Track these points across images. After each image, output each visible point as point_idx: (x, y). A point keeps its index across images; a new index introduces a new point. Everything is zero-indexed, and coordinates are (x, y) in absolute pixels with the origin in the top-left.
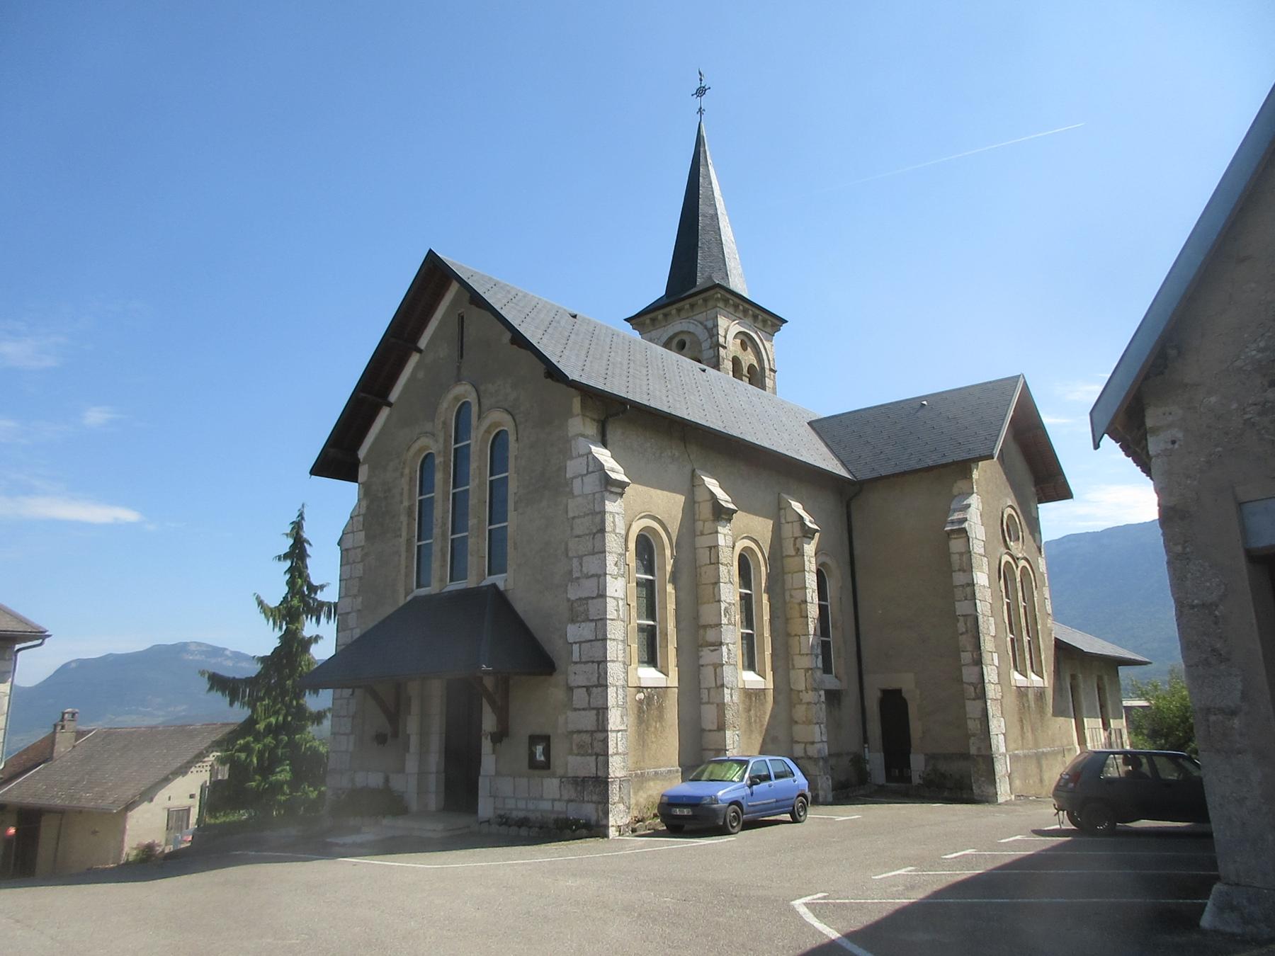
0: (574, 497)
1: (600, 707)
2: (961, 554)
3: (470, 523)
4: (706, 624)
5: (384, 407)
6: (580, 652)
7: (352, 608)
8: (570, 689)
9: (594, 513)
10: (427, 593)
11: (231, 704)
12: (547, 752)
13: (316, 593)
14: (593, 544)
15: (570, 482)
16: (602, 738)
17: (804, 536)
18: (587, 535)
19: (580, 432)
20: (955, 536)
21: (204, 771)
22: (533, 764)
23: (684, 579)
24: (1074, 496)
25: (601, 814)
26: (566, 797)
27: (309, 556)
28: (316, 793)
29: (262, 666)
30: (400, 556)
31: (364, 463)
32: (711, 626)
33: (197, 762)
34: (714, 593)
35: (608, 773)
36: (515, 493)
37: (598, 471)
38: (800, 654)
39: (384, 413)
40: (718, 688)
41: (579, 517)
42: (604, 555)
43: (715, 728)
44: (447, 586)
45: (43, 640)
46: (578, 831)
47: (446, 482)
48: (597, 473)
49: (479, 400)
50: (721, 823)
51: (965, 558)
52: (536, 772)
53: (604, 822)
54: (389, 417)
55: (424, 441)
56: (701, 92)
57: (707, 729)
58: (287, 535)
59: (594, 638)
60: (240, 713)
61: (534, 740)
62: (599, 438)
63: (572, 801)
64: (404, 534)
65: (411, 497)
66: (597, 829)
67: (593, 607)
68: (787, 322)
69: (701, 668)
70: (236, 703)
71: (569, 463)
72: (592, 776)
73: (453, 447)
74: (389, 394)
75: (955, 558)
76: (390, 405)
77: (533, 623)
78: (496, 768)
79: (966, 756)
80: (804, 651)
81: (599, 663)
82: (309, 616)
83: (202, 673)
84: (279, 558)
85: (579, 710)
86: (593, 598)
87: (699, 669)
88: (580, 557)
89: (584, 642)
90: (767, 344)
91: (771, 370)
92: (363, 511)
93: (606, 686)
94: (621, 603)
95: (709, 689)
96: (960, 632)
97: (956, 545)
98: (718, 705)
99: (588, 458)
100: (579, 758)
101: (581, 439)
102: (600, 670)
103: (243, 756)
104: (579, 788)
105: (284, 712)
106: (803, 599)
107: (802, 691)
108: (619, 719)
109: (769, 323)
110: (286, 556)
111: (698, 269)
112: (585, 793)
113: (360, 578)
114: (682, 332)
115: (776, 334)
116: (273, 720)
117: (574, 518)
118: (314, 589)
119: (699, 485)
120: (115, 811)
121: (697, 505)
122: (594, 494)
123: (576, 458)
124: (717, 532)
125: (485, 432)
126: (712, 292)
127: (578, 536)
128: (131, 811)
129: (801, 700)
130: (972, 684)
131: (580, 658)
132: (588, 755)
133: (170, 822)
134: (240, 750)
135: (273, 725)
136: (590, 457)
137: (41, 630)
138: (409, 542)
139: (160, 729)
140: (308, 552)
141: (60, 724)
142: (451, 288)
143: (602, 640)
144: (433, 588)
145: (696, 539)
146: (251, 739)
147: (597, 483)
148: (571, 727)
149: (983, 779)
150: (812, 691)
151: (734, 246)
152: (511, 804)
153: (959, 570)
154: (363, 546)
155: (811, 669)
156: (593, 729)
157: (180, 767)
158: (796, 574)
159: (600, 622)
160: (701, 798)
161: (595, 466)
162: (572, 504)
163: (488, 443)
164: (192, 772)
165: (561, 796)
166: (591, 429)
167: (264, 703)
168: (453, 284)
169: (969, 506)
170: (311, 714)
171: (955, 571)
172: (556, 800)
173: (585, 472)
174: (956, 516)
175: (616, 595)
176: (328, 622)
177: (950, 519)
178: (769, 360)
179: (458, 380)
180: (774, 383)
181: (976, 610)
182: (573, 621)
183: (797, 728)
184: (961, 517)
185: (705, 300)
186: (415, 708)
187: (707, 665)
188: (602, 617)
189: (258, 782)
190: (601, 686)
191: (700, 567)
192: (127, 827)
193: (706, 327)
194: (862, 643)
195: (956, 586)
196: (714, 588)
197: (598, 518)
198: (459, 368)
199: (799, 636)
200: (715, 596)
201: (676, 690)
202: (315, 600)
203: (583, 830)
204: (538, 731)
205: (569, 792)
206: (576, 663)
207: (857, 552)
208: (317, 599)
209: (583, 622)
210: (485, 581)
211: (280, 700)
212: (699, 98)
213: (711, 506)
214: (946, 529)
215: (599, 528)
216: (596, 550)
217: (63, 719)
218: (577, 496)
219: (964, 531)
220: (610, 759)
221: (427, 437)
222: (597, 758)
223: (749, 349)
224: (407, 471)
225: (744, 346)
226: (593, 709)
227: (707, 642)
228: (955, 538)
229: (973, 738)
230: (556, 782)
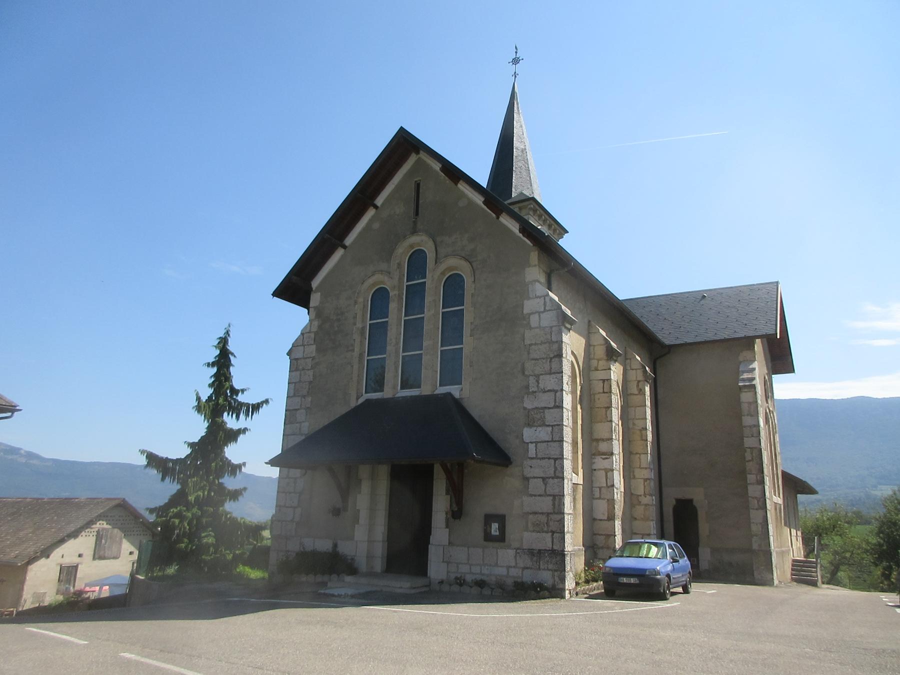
0: (531, 328)
2: (750, 403)
5: (340, 248)
6: (536, 450)
9: (551, 342)
10: (380, 397)
11: (163, 479)
12: (502, 529)
13: (237, 395)
16: (558, 519)
18: (544, 359)
19: (536, 279)
20: (746, 390)
21: (91, 536)
22: (488, 537)
25: (557, 579)
26: (522, 565)
28: (232, 555)
29: (191, 450)
30: (352, 366)
31: (316, 292)
32: (603, 440)
33: (87, 528)
34: (606, 414)
36: (471, 323)
38: (640, 468)
39: (339, 253)
40: (608, 487)
41: (536, 344)
43: (606, 518)
44: (398, 393)
45: (13, 413)
46: (542, 593)
47: (400, 310)
48: (554, 311)
49: (436, 248)
50: (662, 591)
52: (491, 544)
53: (561, 586)
54: (342, 257)
55: (378, 277)
56: (516, 61)
57: (598, 518)
59: (550, 440)
61: (489, 519)
63: (527, 568)
64: (357, 349)
65: (363, 321)
66: (556, 592)
67: (549, 416)
68: (567, 232)
69: (594, 472)
70: (167, 478)
71: (525, 302)
72: (548, 549)
74: (345, 238)
75: (745, 407)
76: (345, 247)
77: (488, 425)
79: (750, 550)
80: (644, 465)
81: (555, 459)
82: (231, 413)
84: (208, 365)
85: (535, 496)
86: (549, 408)
87: (592, 472)
88: (537, 377)
89: (540, 442)
92: (314, 329)
93: (563, 478)
95: (600, 488)
96: (747, 460)
97: (745, 397)
98: (608, 500)
99: (545, 299)
100: (534, 534)
101: (537, 283)
104: (535, 559)
105: (207, 488)
106: (644, 427)
107: (641, 495)
110: (213, 364)
111: (513, 186)
112: (541, 562)
113: (310, 382)
115: (560, 240)
116: (200, 493)
117: (531, 345)
118: (235, 392)
120: (19, 564)
121: (592, 348)
122: (551, 327)
123: (533, 298)
124: (610, 369)
125: (441, 273)
126: (527, 203)
127: (536, 359)
128: (31, 565)
129: (640, 502)
132: (543, 532)
133: (62, 575)
136: (547, 299)
137: (13, 405)
138: (361, 355)
139: (45, 500)
140: (232, 362)
142: (408, 161)
143: (558, 441)
145: (591, 372)
149: (762, 568)
150: (649, 496)
152: (464, 569)
153: (748, 415)
154: (314, 357)
155: (649, 479)
156: (549, 511)
157: (73, 532)
158: (638, 408)
159: (557, 427)
160: (645, 570)
161: (552, 306)
162: (528, 334)
164: (82, 536)
165: (516, 564)
166: (543, 279)
167: (193, 479)
168: (410, 158)
169: (754, 369)
170: (229, 491)
171: (744, 415)
173: (542, 310)
174: (745, 376)
176: (246, 419)
179: (414, 232)
181: (760, 444)
182: (529, 425)
183: (636, 523)
184: (750, 376)
188: (558, 423)
189: (186, 544)
190: (558, 477)
191: (594, 394)
192: (27, 578)
194: (662, 464)
195: (745, 427)
196: (606, 411)
197: (555, 346)
198: (415, 223)
199: (640, 454)
200: (607, 417)
201: (581, 486)
202: (236, 400)
203: (546, 592)
207: (659, 397)
208: (238, 400)
209: (540, 426)
212: (514, 65)
213: (605, 349)
214: (740, 384)
215: (556, 354)
216: (553, 371)
219: (754, 385)
221: (382, 273)
222: (553, 535)
224: (361, 300)
226: (550, 495)
227: (599, 452)
229: (754, 537)
230: (511, 552)
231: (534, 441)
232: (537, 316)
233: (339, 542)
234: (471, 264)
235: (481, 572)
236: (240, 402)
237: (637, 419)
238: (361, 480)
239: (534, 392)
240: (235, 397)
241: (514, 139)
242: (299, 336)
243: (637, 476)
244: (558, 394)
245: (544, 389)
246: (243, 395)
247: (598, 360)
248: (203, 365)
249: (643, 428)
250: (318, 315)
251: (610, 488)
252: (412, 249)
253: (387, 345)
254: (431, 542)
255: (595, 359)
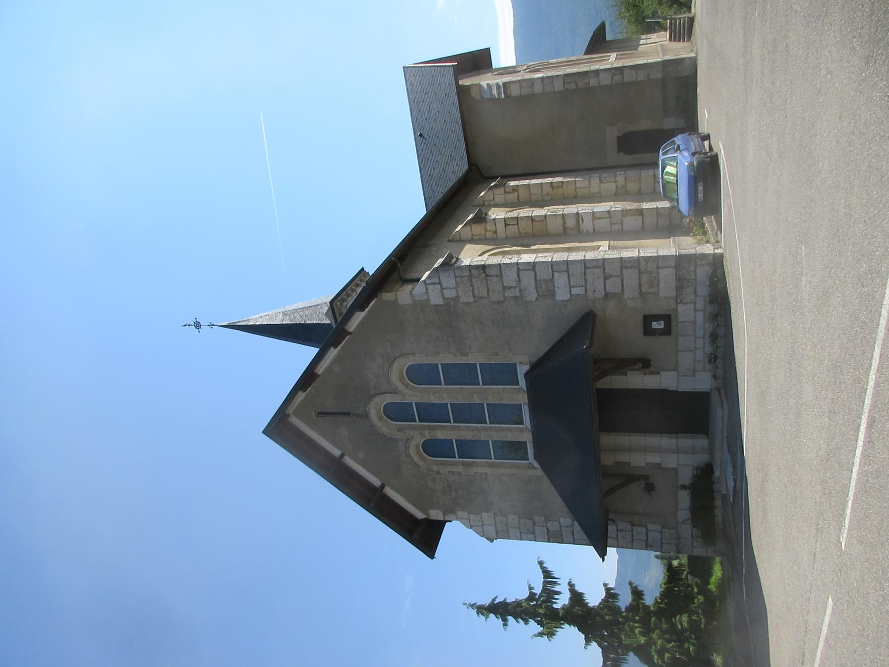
0: (458, 297)
1: (620, 266)
2: (521, 87)
3: (477, 401)
4: (562, 227)
5: (383, 491)
6: (578, 287)
7: (543, 526)
8: (607, 295)
9: (471, 276)
10: (532, 445)
12: (657, 318)
13: (536, 594)
14: (494, 276)
15: (447, 301)
17: (504, 185)
18: (487, 283)
19: (409, 294)
22: (667, 331)
23: (526, 241)
24: (488, 47)
25: (704, 262)
26: (692, 297)
27: (505, 600)
28: (699, 596)
29: (593, 642)
30: (502, 474)
31: (428, 514)
32: (564, 223)
34: (539, 221)
35: (672, 256)
36: (455, 356)
37: (439, 274)
38: (589, 188)
40: (610, 216)
41: (473, 291)
42: (502, 265)
44: (526, 427)
46: (718, 276)
47: (444, 428)
48: (440, 275)
49: (381, 394)
50: (709, 159)
51: (524, 84)
52: (673, 329)
53: (711, 258)
54: (393, 488)
55: (412, 452)
56: (198, 325)
58: (486, 618)
59: (566, 273)
61: (648, 331)
63: (695, 291)
65: (456, 464)
66: (717, 264)
67: (543, 275)
68: (363, 269)
69: (596, 231)
72: (675, 272)
73: (418, 423)
75: (525, 91)
76: (383, 486)
77: (555, 336)
78: (671, 371)
80: (587, 184)
81: (586, 267)
82: (554, 601)
84: (505, 625)
86: (536, 275)
88: (505, 288)
92: (465, 514)
93: (604, 260)
95: (612, 224)
97: (515, 91)
98: (623, 216)
99: (428, 284)
101: (413, 292)
102: (591, 266)
105: (631, 623)
106: (549, 185)
107: (617, 186)
109: (362, 278)
110: (505, 620)
112: (688, 278)
113: (520, 517)
116: (637, 631)
117: (474, 296)
118: (532, 597)
119: (460, 235)
122: (456, 276)
125: (407, 387)
126: (336, 311)
130: (612, 77)
131: (582, 287)
132: (659, 277)
135: (643, 630)
136: (428, 282)
138: (491, 466)
140: (502, 600)
143: (567, 265)
147: (447, 274)
148: (636, 294)
149: (679, 68)
150: (616, 177)
152: (700, 355)
153: (532, 88)
154: (494, 515)
155: (600, 178)
156: (637, 272)
158: (531, 192)
159: (553, 268)
160: (689, 177)
161: (435, 276)
162: (463, 299)
163: (416, 387)
165: (692, 303)
166: (409, 287)
167: (623, 639)
169: (488, 84)
171: (533, 91)
172: (695, 307)
173: (439, 286)
174: (495, 92)
176: (559, 584)
177: (496, 96)
179: (366, 416)
181: (561, 75)
182: (553, 295)
184: (495, 88)
186: (624, 458)
187: (593, 225)
188: (550, 265)
189: (690, 645)
190: (604, 265)
191: (520, 233)
195: (544, 91)
196: (535, 221)
197: (474, 272)
198: (357, 416)
199: (576, 188)
200: (541, 220)
201: (611, 242)
204: (640, 329)
206: (586, 291)
207: (519, 172)
209: (554, 284)
210: (523, 388)
211: (621, 626)
212: (202, 327)
215: (482, 271)
216: (499, 274)
218: (457, 293)
221: (409, 447)
224: (435, 468)
227: (576, 226)
228: (510, 91)
230: (680, 308)
231: (568, 289)
232: (444, 291)
233: (680, 483)
234: (397, 358)
235: (701, 338)
236: (542, 591)
237: (542, 192)
238: (616, 462)
239: (520, 291)
240: (537, 597)
241: (274, 323)
242: (473, 530)
243: (597, 190)
244: (521, 267)
245: (516, 281)
246: (535, 588)
247: (486, 231)
248: (506, 630)
249: (551, 186)
251: (611, 214)
252: (383, 417)
253: (479, 439)
254: (676, 389)
255: (485, 234)
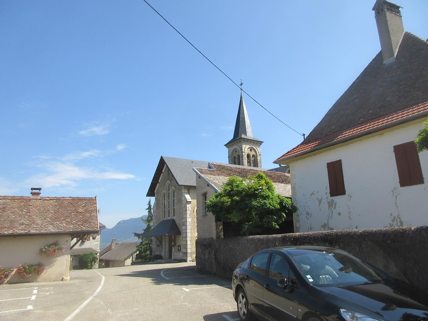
8: (183, 238)
9: (185, 207)
11: (139, 239)
12: (180, 248)
60: (140, 240)
62: (188, 192)
64: (162, 208)
76: (159, 183)
83: (133, 233)
88: (184, 215)
90: (258, 149)
91: (259, 155)
94: (190, 222)
103: (141, 249)
105: (148, 240)
108: (190, 243)
110: (148, 209)
114: (236, 148)
134: (140, 248)
138: (162, 209)
141: (112, 242)
144: (165, 219)
146: (142, 246)
148: (183, 244)
151: (249, 125)
157: (135, 251)
175: (189, 221)
178: (258, 152)
180: (261, 158)
182: (183, 226)
185: (240, 141)
193: (240, 148)
198: (168, 177)
204: (179, 245)
205: (183, 255)
217: (113, 241)
220: (188, 249)
223: (253, 151)
224: (162, 196)
225: (251, 150)
233: (161, 252)
250: (156, 199)
